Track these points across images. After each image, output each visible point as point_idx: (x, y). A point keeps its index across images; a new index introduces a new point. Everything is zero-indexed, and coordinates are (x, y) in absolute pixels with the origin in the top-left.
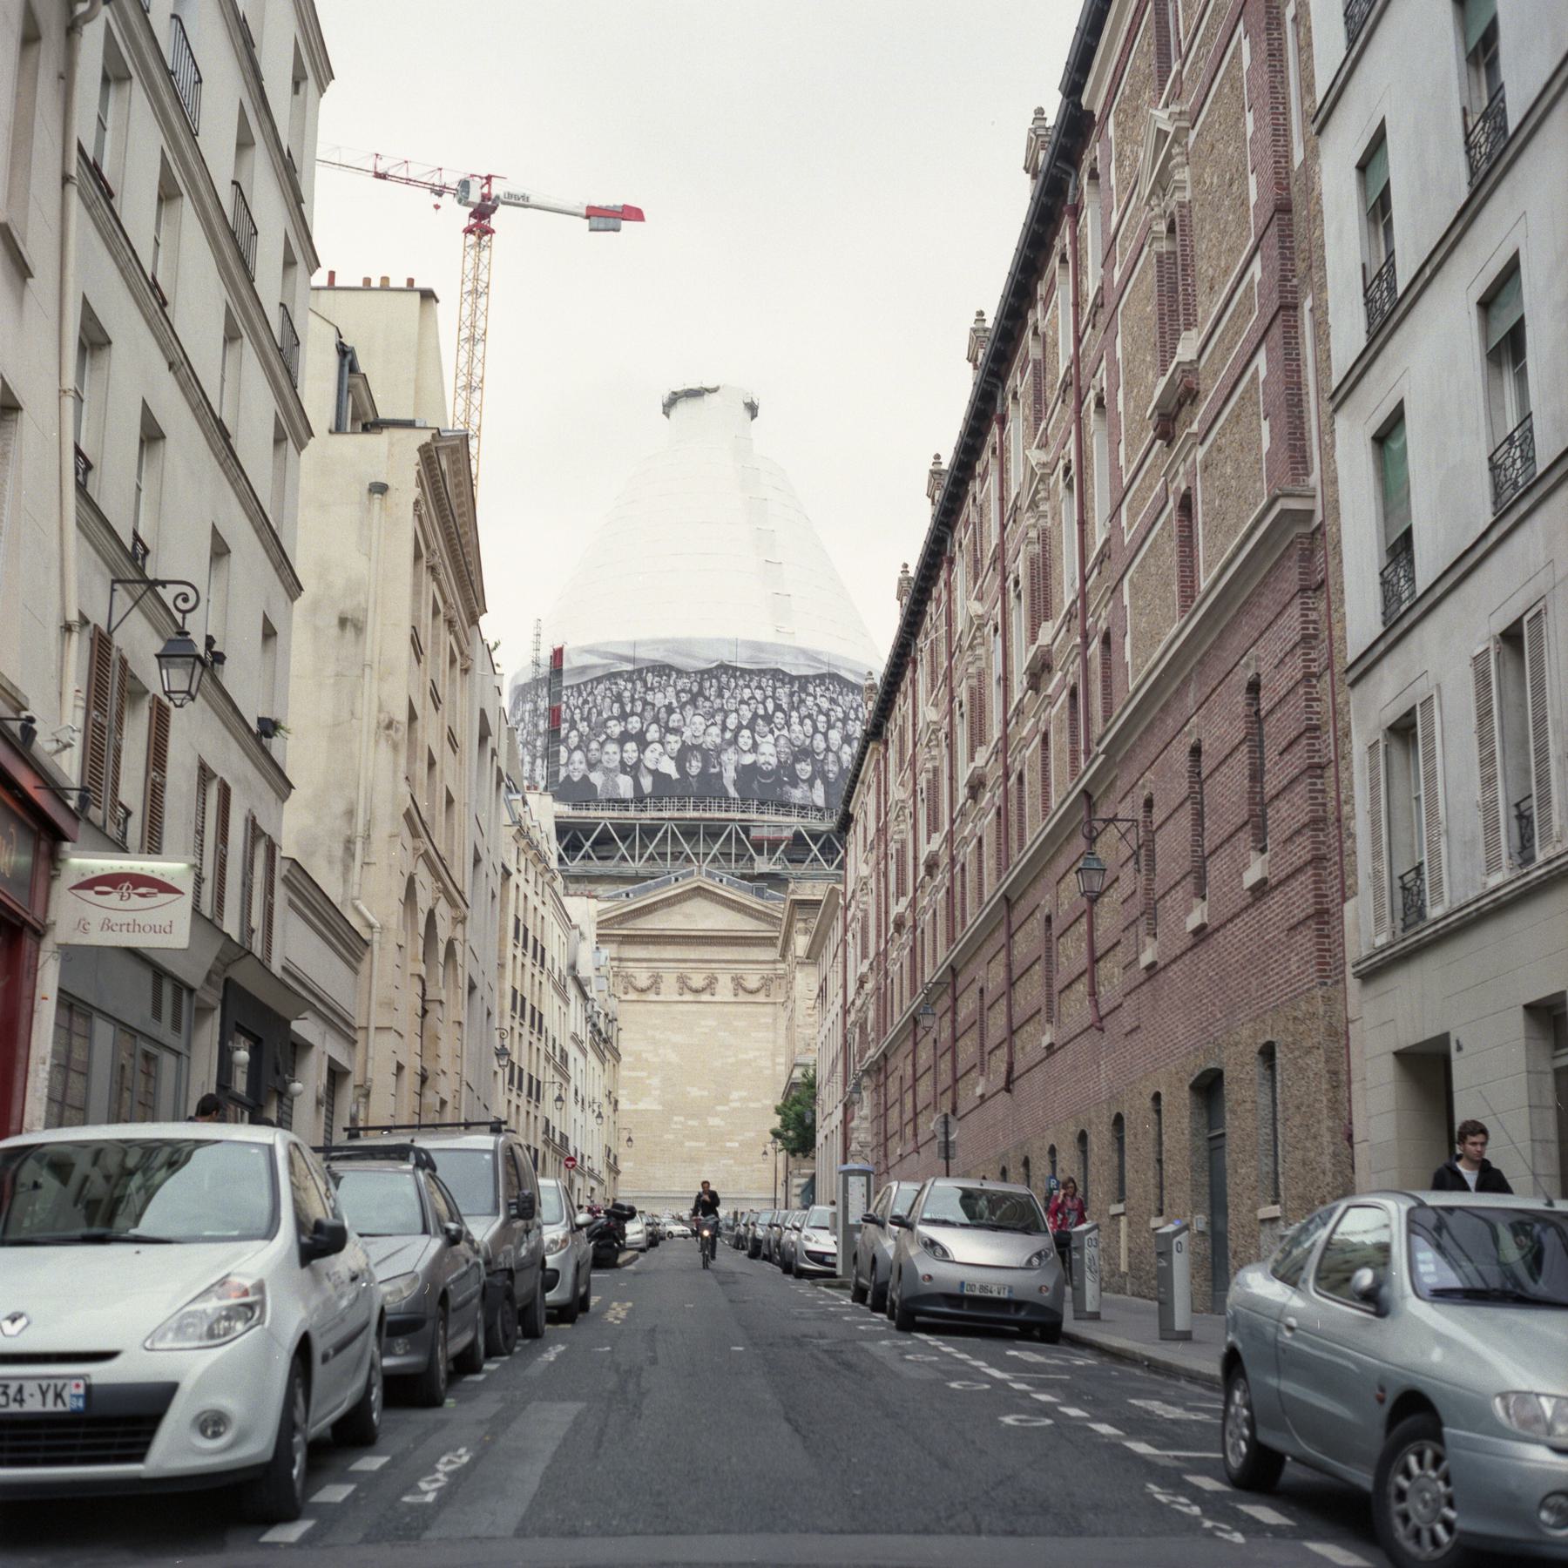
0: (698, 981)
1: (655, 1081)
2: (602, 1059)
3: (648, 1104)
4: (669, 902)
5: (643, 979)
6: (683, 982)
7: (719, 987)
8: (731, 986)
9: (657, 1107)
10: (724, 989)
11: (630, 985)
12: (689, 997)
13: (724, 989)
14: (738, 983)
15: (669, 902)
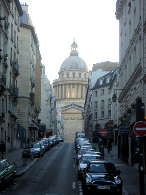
0: (73, 118)
1: (68, 131)
2: (62, 129)
3: (67, 134)
4: (69, 109)
5: (66, 118)
6: (71, 119)
7: (76, 119)
8: (77, 119)
9: (68, 134)
10: (76, 120)
11: (64, 119)
12: (72, 120)
13: (76, 120)
14: (78, 119)
15: (69, 109)
